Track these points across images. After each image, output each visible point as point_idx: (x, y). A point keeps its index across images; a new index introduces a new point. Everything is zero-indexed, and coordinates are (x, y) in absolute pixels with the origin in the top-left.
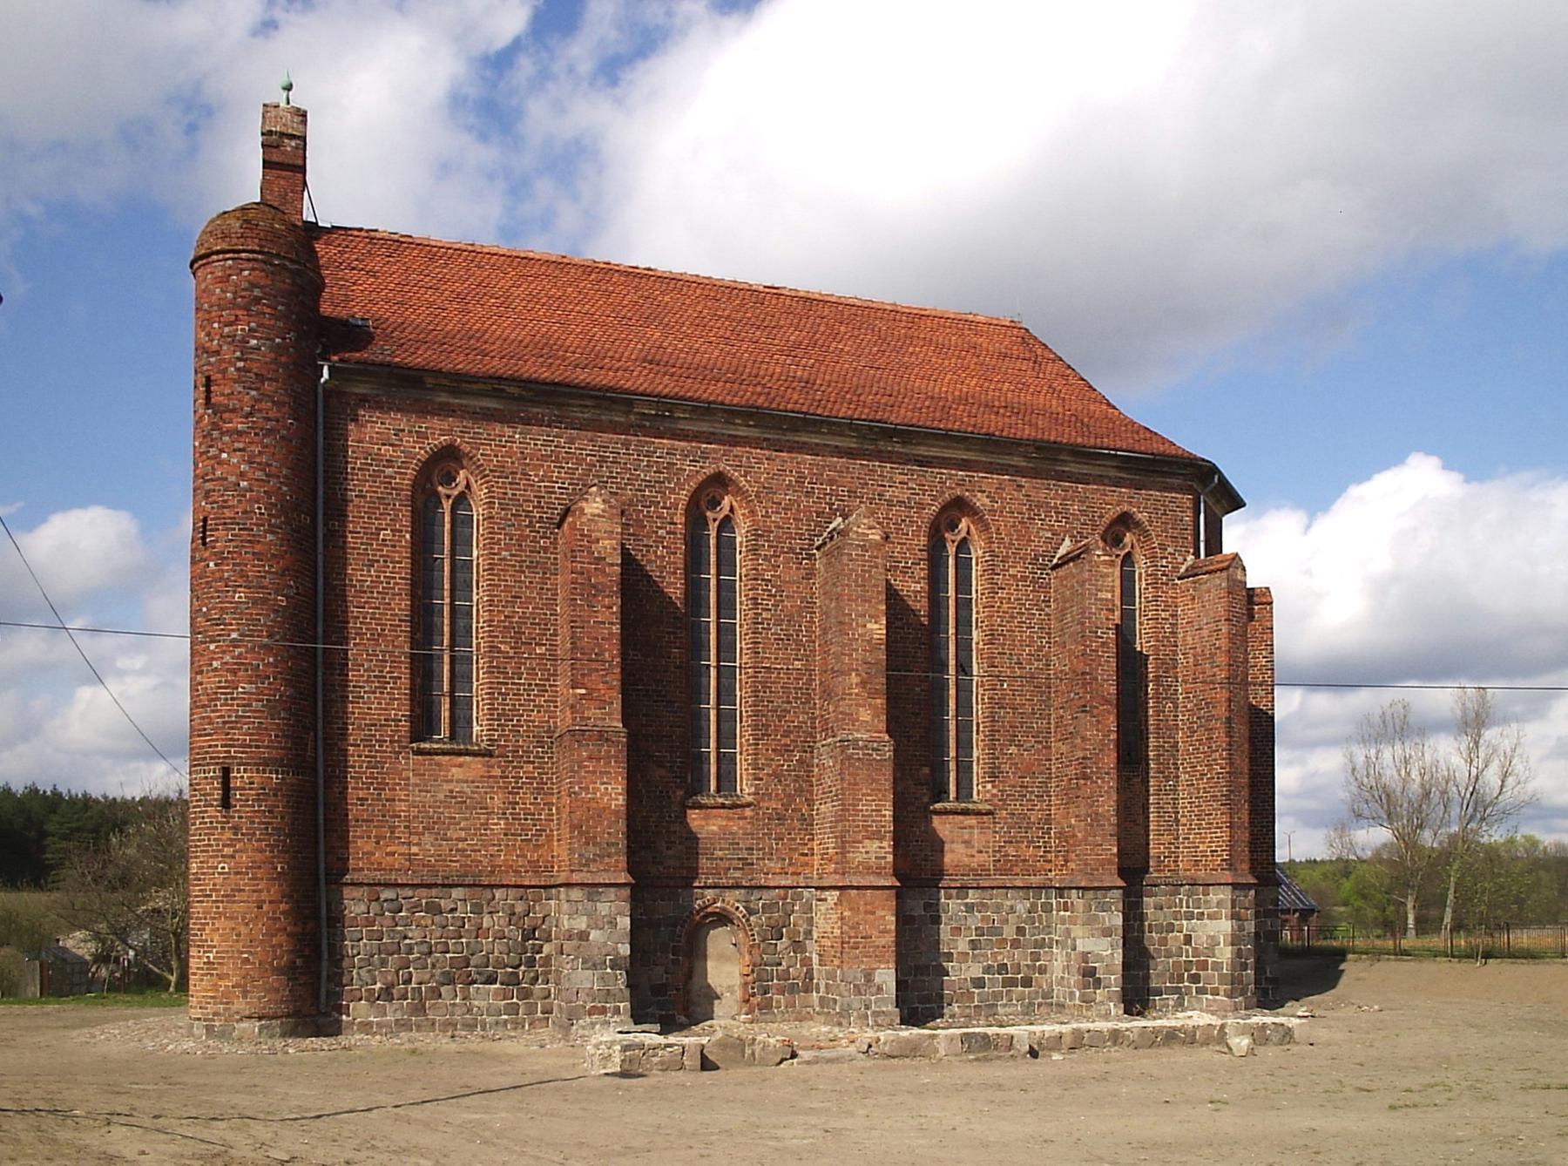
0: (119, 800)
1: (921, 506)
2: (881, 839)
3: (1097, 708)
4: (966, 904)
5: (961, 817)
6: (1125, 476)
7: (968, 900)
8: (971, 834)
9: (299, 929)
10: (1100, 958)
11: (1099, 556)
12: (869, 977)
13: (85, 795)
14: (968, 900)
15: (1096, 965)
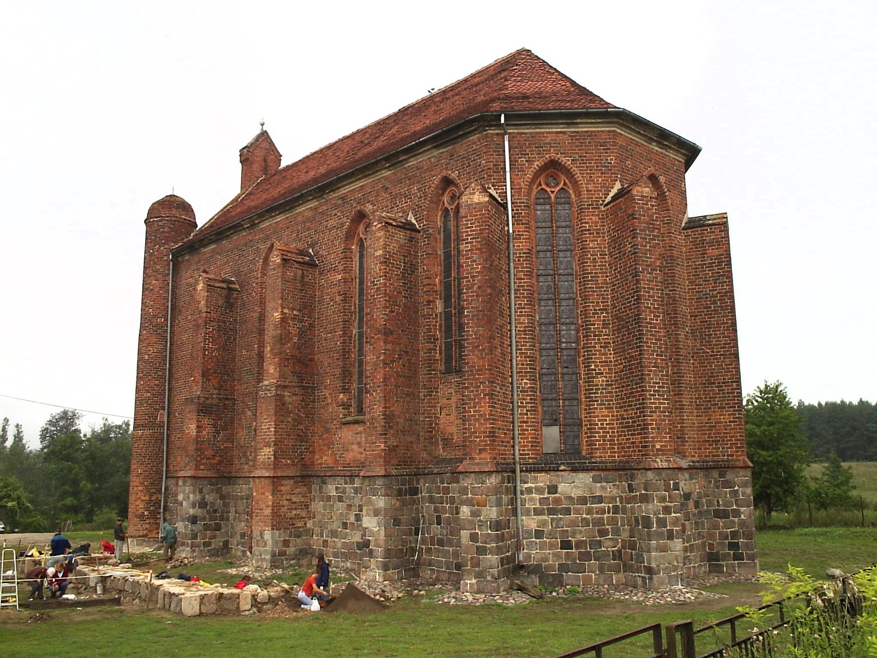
0: (823, 403)
1: (342, 225)
2: (270, 447)
3: (373, 338)
4: (354, 488)
5: (356, 426)
6: (444, 150)
7: (355, 485)
8: (361, 437)
9: (147, 498)
10: (372, 534)
11: (376, 226)
12: (262, 535)
13: (842, 402)
14: (355, 485)
15: (370, 538)
